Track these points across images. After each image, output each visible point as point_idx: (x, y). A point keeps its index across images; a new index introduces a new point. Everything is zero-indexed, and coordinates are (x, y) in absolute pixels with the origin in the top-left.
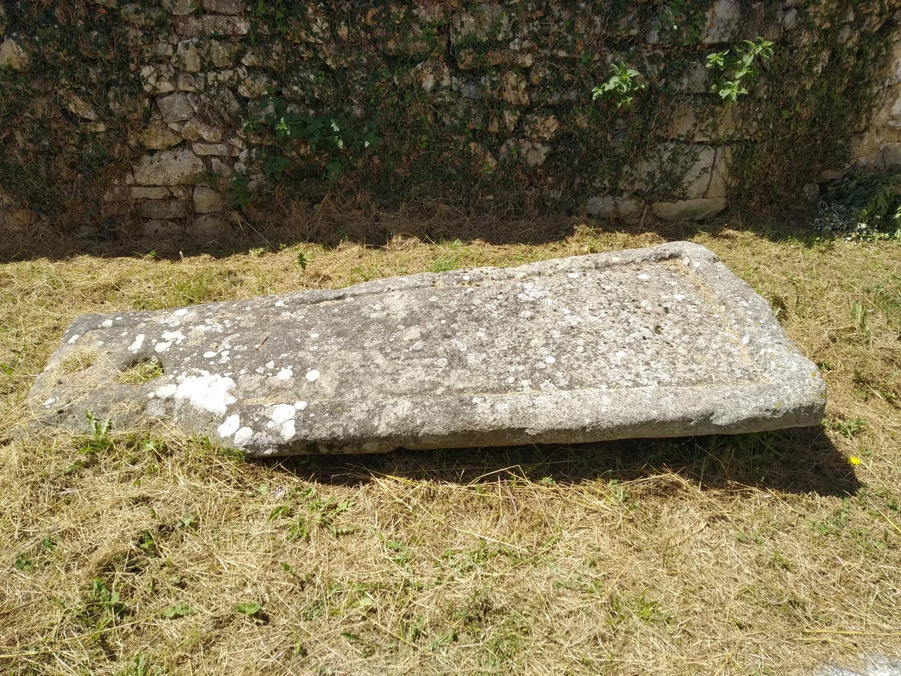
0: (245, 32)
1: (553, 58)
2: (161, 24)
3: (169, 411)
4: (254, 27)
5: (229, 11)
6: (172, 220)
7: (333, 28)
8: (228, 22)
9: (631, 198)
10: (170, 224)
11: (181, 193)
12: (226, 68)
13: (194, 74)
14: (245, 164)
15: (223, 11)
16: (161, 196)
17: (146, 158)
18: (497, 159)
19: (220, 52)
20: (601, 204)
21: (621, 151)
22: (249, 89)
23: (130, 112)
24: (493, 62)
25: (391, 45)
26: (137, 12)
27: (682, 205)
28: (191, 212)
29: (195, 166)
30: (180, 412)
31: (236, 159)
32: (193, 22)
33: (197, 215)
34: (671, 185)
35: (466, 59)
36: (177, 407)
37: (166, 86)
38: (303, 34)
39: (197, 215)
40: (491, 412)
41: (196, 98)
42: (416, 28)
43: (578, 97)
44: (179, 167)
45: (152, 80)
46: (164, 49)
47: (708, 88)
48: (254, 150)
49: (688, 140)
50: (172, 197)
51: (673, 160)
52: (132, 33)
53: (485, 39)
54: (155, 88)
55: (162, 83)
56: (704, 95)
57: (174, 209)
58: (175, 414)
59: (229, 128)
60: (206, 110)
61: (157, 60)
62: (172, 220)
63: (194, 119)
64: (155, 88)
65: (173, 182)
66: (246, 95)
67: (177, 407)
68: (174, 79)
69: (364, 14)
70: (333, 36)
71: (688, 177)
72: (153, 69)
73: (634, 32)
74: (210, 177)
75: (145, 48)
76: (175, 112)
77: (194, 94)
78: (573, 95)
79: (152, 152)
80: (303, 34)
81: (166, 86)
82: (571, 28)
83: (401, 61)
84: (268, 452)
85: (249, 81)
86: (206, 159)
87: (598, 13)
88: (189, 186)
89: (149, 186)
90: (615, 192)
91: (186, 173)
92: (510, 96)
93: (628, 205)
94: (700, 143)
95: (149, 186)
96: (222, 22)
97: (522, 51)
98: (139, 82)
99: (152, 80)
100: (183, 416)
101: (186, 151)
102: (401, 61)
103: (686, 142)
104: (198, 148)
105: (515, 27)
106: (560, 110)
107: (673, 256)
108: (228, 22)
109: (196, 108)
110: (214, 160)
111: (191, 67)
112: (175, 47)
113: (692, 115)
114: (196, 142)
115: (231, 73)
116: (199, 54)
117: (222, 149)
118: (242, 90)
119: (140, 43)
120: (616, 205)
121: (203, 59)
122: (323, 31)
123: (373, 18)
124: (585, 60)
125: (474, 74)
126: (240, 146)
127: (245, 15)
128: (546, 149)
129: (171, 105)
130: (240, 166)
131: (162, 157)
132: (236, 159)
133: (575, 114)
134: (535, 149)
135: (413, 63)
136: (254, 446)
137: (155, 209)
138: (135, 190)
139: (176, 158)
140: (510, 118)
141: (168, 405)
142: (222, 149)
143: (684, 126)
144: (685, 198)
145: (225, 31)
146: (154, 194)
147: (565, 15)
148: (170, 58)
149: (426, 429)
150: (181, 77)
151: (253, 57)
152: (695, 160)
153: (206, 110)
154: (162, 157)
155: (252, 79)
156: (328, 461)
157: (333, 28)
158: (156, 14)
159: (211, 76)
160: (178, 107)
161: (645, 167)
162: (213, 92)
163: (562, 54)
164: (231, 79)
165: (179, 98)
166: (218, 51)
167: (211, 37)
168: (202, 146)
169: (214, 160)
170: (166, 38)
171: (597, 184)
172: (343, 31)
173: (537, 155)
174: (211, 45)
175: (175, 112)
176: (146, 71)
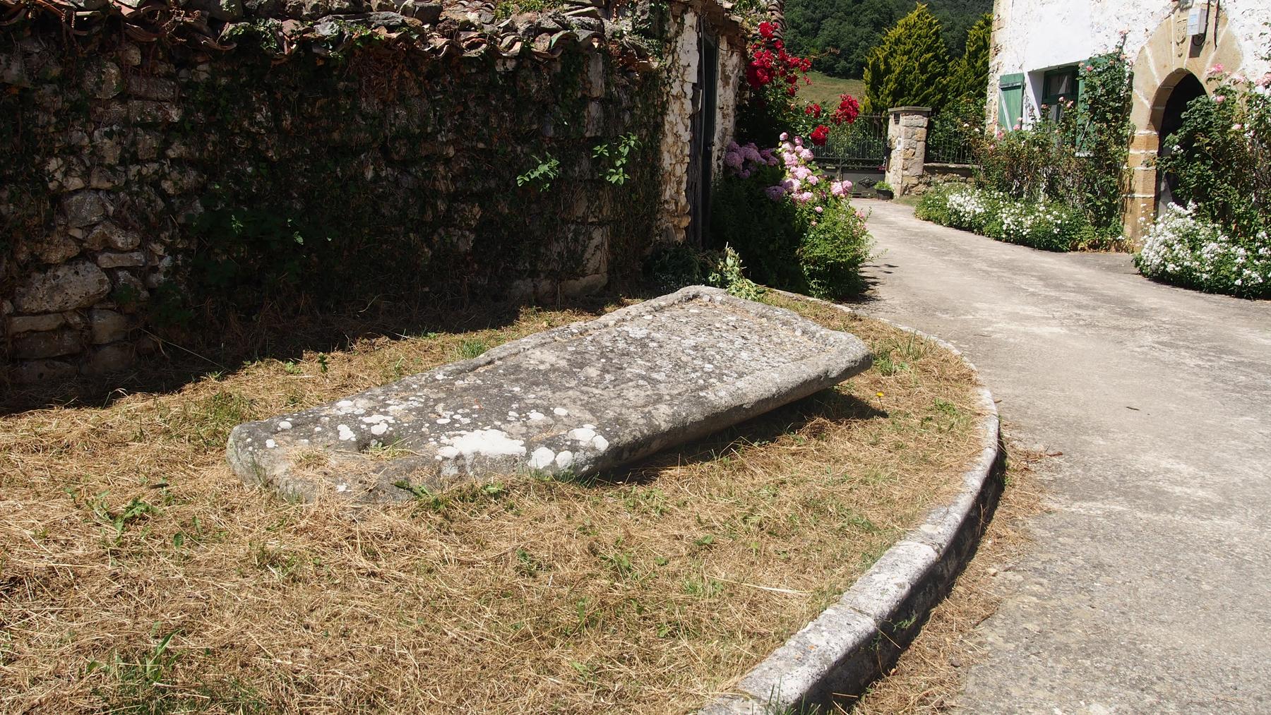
0: (176, 119)
1: (474, 149)
2: (77, 108)
3: (461, 468)
4: (187, 114)
5: (160, 95)
6: (61, 358)
7: (277, 118)
8: (158, 109)
9: (546, 277)
10: (57, 363)
11: (77, 319)
12: (153, 161)
13: (111, 167)
14: (166, 275)
15: (154, 96)
16: (55, 325)
17: (38, 276)
18: (431, 248)
19: (148, 141)
20: (523, 286)
21: (538, 233)
22: (175, 184)
23: (30, 217)
24: (424, 153)
25: (336, 135)
26: (55, 93)
27: (584, 281)
28: (91, 345)
29: (101, 282)
30: (473, 467)
31: (155, 269)
32: (116, 108)
33: (97, 347)
34: (573, 264)
35: (402, 149)
36: (468, 463)
37: (75, 183)
38: (246, 124)
39: (97, 347)
40: (721, 395)
41: (112, 196)
42: (359, 119)
43: (498, 185)
44: (83, 284)
45: (58, 175)
46: (77, 136)
47: (593, 175)
48: (180, 257)
49: (584, 222)
50: (66, 327)
51: (576, 240)
52: (42, 118)
53: (417, 131)
54: (61, 186)
55: (71, 180)
56: (592, 180)
57: (68, 340)
58: (468, 469)
59: (150, 231)
60: (125, 211)
61: (72, 150)
62: (61, 358)
63: (107, 223)
64: (61, 186)
65: (71, 305)
66: (171, 191)
67: (468, 463)
68: (86, 175)
69: (312, 105)
70: (276, 126)
71: (587, 255)
72: (61, 162)
73: (535, 127)
74: (113, 298)
75: (57, 136)
76: (84, 214)
77: (108, 192)
78: (493, 184)
79: (48, 266)
80: (246, 124)
81: (75, 183)
82: (486, 122)
83: (344, 152)
84: (585, 469)
85: (175, 175)
86: (110, 272)
87: (506, 109)
88: (86, 310)
89: (38, 314)
90: (534, 274)
91: (92, 291)
92: (441, 186)
93: (545, 285)
94: (592, 223)
95: (38, 314)
96: (151, 108)
97: (448, 143)
98: (41, 177)
99: (58, 175)
100: (478, 469)
101: (88, 264)
102: (344, 152)
103: (583, 223)
104: (105, 260)
105: (441, 121)
106: (484, 198)
107: (695, 297)
108: (158, 109)
109: (111, 209)
110: (120, 274)
111: (111, 159)
112: (91, 135)
113: (585, 199)
114: (102, 252)
115: (156, 166)
116: (121, 144)
117: (138, 257)
118: (167, 185)
119: (52, 130)
120: (535, 286)
121: (124, 150)
122: (267, 121)
123: (321, 108)
124: (501, 151)
125: (404, 165)
126: (161, 253)
127: (178, 102)
128: (472, 237)
129: (80, 205)
130: (158, 278)
131: (59, 273)
132: (155, 269)
133: (498, 201)
134: (465, 237)
135: (356, 154)
136: (575, 467)
137: (43, 345)
138: (17, 321)
139: (77, 273)
140: (442, 206)
141: (460, 462)
142: (138, 257)
143: (580, 210)
144: (584, 275)
145: (155, 118)
146: (46, 323)
147: (480, 110)
148: (82, 148)
149: (690, 418)
150: (96, 171)
151: (183, 148)
152: (591, 238)
153: (125, 211)
154: (59, 273)
155: (180, 173)
156: (632, 463)
157: (277, 118)
158: (75, 96)
159: (134, 169)
160: (88, 208)
161: (557, 248)
162: (135, 189)
163: (481, 145)
164: (156, 172)
165: (91, 197)
166: (144, 140)
167: (137, 124)
168: (113, 256)
169: (120, 274)
170: (83, 125)
171: (520, 267)
172: (287, 122)
173: (466, 243)
174: (136, 134)
175: (84, 214)
176: (53, 164)
